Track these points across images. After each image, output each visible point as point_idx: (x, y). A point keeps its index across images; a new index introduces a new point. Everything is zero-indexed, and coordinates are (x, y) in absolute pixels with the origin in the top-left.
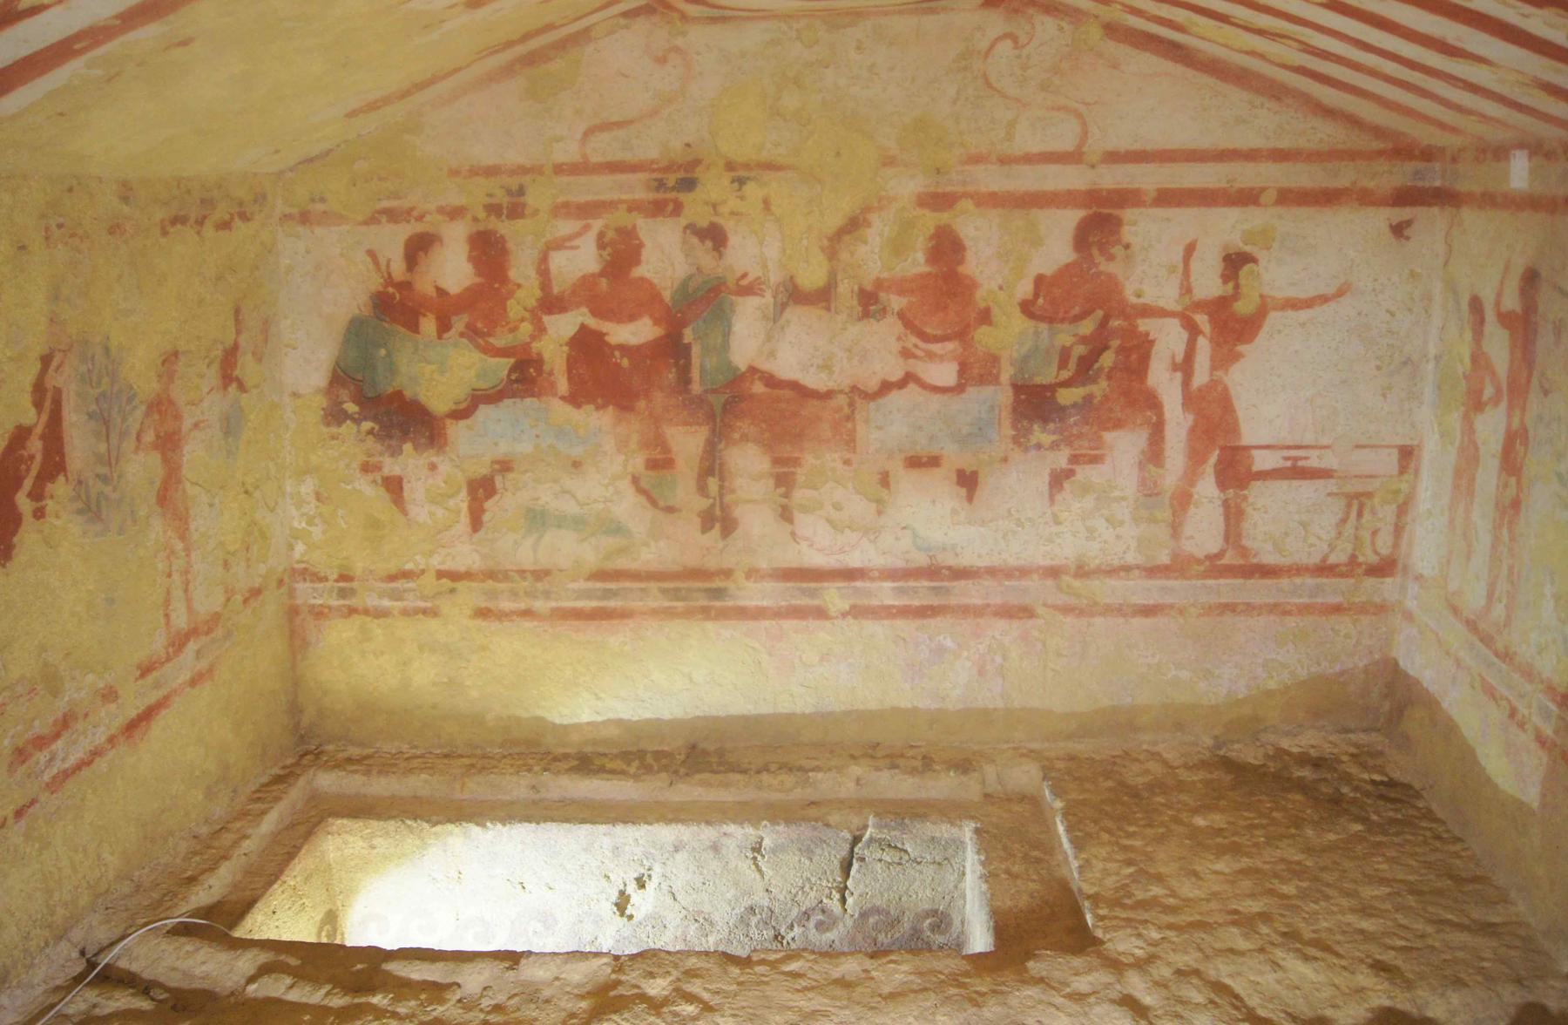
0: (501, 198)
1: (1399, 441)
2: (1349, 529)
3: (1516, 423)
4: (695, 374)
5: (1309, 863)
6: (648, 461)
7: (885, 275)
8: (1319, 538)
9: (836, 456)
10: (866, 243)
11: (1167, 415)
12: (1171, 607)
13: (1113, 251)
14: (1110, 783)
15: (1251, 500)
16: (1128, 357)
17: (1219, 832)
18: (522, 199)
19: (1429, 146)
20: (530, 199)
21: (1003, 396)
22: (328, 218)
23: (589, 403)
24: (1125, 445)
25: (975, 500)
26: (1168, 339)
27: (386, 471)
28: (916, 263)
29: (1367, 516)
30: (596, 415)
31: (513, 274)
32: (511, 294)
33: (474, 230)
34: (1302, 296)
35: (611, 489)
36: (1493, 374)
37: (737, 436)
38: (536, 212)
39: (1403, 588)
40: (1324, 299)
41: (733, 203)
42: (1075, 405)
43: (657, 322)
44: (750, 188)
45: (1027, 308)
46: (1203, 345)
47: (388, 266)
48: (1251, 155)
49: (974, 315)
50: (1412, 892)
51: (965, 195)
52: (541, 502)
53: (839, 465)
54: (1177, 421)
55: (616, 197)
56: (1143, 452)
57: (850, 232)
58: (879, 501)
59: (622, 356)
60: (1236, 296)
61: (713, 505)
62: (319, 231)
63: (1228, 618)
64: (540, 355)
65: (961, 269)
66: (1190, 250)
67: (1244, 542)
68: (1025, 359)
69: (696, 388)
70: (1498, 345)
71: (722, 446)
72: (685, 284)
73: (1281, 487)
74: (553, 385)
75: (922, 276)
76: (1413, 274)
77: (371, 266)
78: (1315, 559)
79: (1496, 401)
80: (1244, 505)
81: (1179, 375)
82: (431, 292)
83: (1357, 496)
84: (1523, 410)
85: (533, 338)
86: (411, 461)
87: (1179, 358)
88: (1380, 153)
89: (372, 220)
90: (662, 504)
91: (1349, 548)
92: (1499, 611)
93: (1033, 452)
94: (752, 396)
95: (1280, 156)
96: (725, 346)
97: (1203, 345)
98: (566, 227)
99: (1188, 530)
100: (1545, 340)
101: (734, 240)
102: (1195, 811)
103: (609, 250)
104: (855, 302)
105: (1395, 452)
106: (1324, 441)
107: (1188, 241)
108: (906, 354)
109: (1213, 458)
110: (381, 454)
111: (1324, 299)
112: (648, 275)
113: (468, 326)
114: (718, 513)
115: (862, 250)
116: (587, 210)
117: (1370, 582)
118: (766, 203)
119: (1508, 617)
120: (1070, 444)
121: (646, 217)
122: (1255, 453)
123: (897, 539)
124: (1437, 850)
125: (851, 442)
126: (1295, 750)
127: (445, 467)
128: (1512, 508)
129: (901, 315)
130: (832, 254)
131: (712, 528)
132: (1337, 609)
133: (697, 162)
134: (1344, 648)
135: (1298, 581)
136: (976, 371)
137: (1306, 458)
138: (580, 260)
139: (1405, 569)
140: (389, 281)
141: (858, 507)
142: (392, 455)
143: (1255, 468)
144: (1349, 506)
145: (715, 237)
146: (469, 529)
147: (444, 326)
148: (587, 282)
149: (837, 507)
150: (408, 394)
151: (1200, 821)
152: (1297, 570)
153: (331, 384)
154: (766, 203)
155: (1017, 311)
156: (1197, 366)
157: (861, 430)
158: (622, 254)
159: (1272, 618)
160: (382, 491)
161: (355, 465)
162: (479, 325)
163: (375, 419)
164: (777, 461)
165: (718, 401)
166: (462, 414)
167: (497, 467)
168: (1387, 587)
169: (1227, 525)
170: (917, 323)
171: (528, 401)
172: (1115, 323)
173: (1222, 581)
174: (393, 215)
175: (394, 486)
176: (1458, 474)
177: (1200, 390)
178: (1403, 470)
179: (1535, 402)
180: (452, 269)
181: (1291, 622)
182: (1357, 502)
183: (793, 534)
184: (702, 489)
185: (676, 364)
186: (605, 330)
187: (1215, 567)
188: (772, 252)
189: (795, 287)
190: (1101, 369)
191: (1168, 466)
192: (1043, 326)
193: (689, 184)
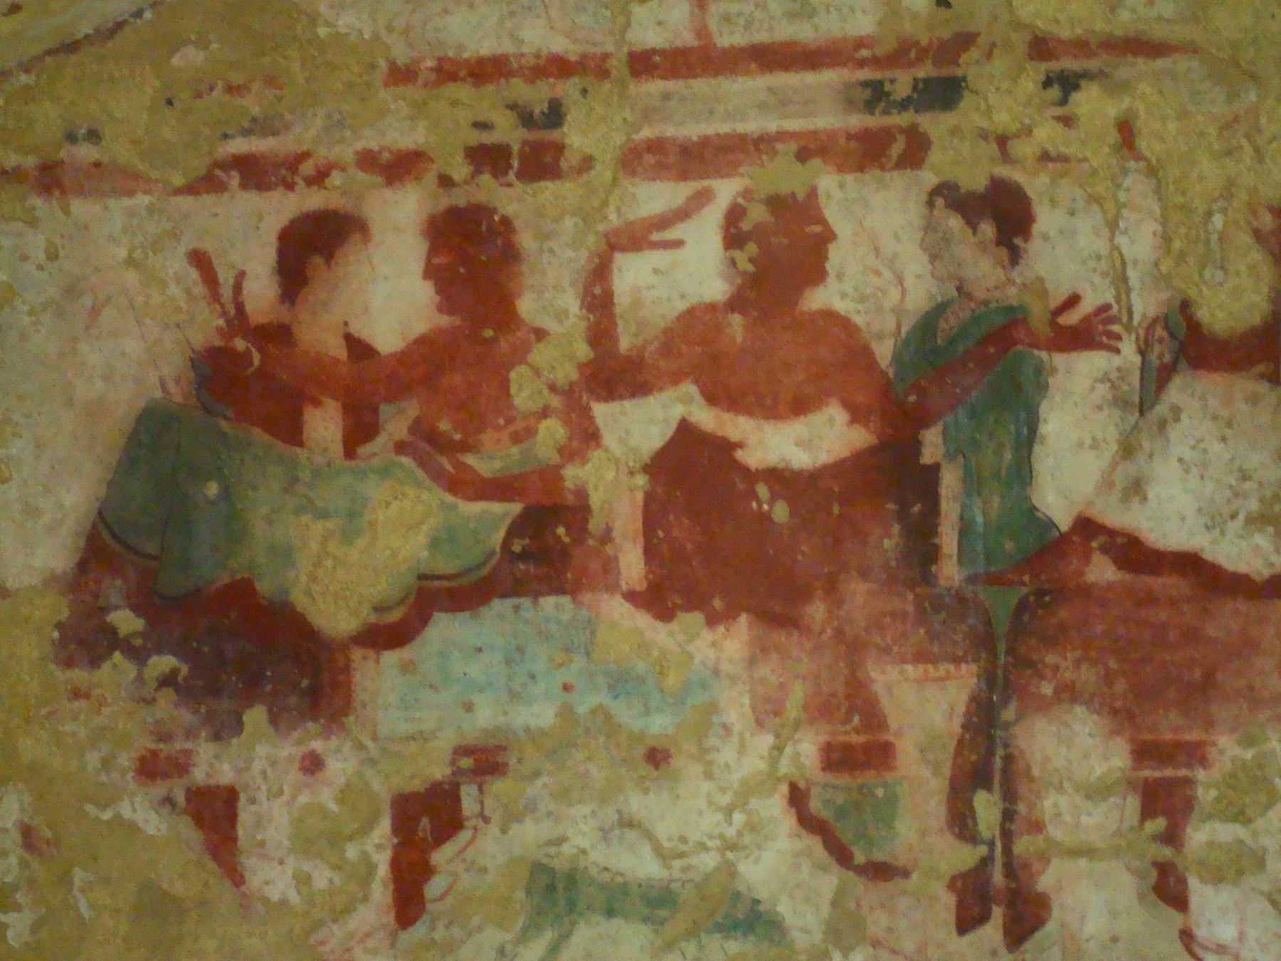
0: (507, 132)
4: (948, 540)
6: (828, 748)
18: (555, 135)
20: (576, 136)
22: (107, 179)
23: (690, 607)
27: (199, 775)
30: (707, 636)
31: (527, 306)
32: (520, 355)
33: (444, 202)
35: (738, 818)
37: (1047, 689)
38: (587, 163)
41: (1046, 133)
43: (857, 415)
44: (1088, 100)
47: (238, 288)
52: (567, 849)
55: (772, 126)
59: (774, 498)
61: (986, 862)
62: (78, 206)
64: (582, 494)
69: (950, 572)
71: (1008, 714)
72: (929, 322)
74: (610, 566)
77: (199, 289)
82: (337, 349)
85: (570, 454)
86: (262, 750)
89: (208, 183)
90: (859, 858)
94: (1087, 592)
96: (1023, 472)
98: (654, 197)
101: (1046, 220)
103: (752, 248)
110: (190, 734)
112: (841, 306)
113: (415, 428)
114: (998, 877)
116: (696, 159)
118: (1126, 130)
121: (841, 169)
127: (341, 766)
131: (983, 918)
133: (965, 40)
138: (686, 272)
140: (238, 320)
142: (217, 737)
145: (1005, 214)
146: (390, 918)
147: (360, 431)
148: (697, 323)
150: (265, 586)
153: (82, 565)
154: (1126, 130)
158: (781, 254)
160: (186, 827)
161: (125, 760)
162: (444, 426)
163: (180, 650)
164: (1144, 752)
165: (1002, 603)
166: (389, 634)
167: (466, 762)
171: (548, 602)
174: (254, 173)
175: (216, 814)
180: (389, 295)
183: (1187, 936)
184: (961, 822)
185: (902, 515)
186: (733, 434)
188: (1140, 244)
189: (1194, 327)
193: (944, 93)
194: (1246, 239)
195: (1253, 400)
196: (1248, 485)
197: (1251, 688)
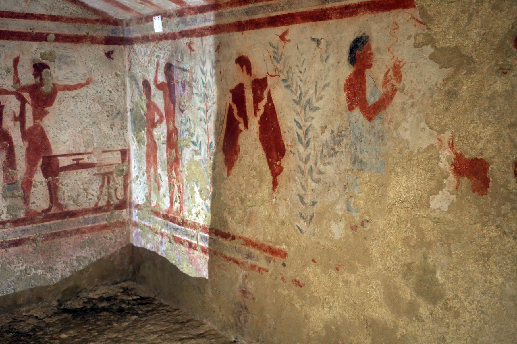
1: (120, 148)
2: (105, 190)
3: (171, 127)
5: (120, 336)
11: (15, 143)
12: (28, 239)
14: (11, 334)
15: (60, 181)
17: (75, 337)
19: (116, 19)
29: (112, 183)
34: (72, 84)
36: (158, 110)
39: (130, 213)
40: (81, 86)
46: (28, 107)
48: (40, 17)
50: (166, 333)
54: (20, 147)
56: (4, 162)
60: (41, 84)
63: (57, 240)
66: (16, 61)
67: (60, 201)
70: (159, 99)
76: (117, 75)
78: (93, 205)
79: (160, 121)
80: (57, 184)
81: (18, 123)
83: (106, 174)
84: (174, 121)
87: (17, 114)
88: (97, 21)
91: (106, 197)
92: (177, 205)
95: (54, 19)
99: (32, 199)
100: (178, 89)
102: (61, 332)
105: (119, 152)
106: (89, 150)
107: (15, 57)
109: (40, 163)
117: (117, 212)
119: (181, 207)
122: (59, 158)
124: (169, 316)
126: (96, 297)
128: (174, 163)
132: (105, 227)
134: (110, 243)
135: (86, 217)
137: (83, 159)
139: (130, 203)
143: (61, 165)
144: (104, 179)
151: (64, 336)
152: (86, 211)
156: (27, 118)
159: (77, 236)
168: (124, 212)
173: (52, 222)
176: (148, 156)
177: (29, 129)
178: (123, 160)
179: (178, 117)
181: (86, 236)
182: (106, 177)
187: (47, 215)
191: (18, 168)
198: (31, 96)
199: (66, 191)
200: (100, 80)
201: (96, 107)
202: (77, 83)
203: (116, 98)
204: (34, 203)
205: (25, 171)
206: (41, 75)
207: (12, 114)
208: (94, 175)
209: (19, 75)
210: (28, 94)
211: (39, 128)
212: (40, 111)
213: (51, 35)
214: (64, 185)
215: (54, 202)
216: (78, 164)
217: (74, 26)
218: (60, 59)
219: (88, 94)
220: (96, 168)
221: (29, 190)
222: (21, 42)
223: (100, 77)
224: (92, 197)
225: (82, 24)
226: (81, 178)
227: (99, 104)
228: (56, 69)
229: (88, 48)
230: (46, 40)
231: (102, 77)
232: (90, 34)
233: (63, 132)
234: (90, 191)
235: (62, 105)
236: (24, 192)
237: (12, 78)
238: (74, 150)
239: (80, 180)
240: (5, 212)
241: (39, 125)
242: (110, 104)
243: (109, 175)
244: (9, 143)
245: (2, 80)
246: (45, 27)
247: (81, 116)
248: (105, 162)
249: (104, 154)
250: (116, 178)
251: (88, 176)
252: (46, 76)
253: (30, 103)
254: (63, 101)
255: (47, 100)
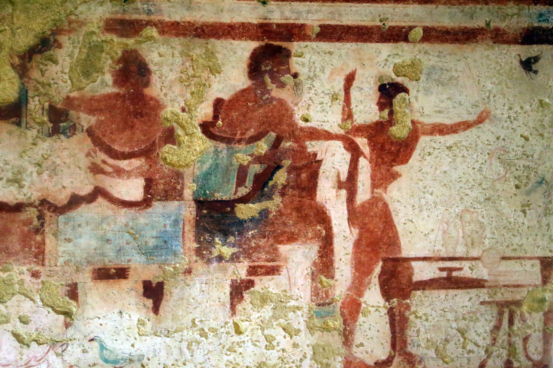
2: (502, 337)
7: (74, 94)
8: (476, 344)
9: (24, 268)
10: (56, 62)
11: (335, 230)
13: (282, 79)
15: (413, 309)
16: (298, 175)
21: (187, 210)
24: (299, 257)
25: (161, 311)
26: (334, 159)
28: (105, 84)
29: (516, 321)
34: (448, 122)
40: (467, 125)
42: (252, 219)
45: (207, 128)
46: (364, 164)
49: (159, 134)
51: (149, 23)
53: (27, 278)
57: (40, 52)
58: (67, 314)
60: (391, 122)
65: (147, 91)
66: (350, 80)
67: (409, 349)
68: (207, 176)
73: (439, 297)
75: (109, 97)
80: (407, 313)
81: (344, 192)
83: (507, 304)
87: (344, 177)
91: (505, 353)
93: (215, 264)
97: (364, 164)
99: (358, 338)
104: (46, 119)
105: (538, 262)
106: (475, 253)
108: (95, 169)
109: (378, 270)
111: (467, 125)
115: (53, 69)
120: (249, 256)
122: (414, 264)
123: (84, 351)
125: (40, 255)
129: (90, 132)
130: (22, 71)
136: (160, 189)
137: (460, 269)
141: (47, 320)
143: (417, 277)
144: (501, 314)
149: (24, 321)
155: (198, 132)
156: (359, 184)
157: (50, 241)
169: (393, 332)
170: (106, 140)
172: (287, 144)
177: (363, 206)
182: (507, 311)
190: (274, 186)
191: (337, 275)
192: (222, 146)
194: (9, 68)
195: (10, 133)
196: (7, 166)
197: (7, 248)
198: (369, 144)
199: (422, 330)
200: (506, 116)
201: (493, 167)
202: (459, 120)
203: (537, 152)
204: (362, 345)
205: (349, 283)
206: (391, 105)
207: (335, 175)
208: (482, 303)
209: (353, 106)
210: (365, 140)
211: (380, 205)
212: (383, 171)
213: (416, 29)
214: (421, 318)
215: (398, 348)
216: (449, 279)
217: (462, 11)
218: (429, 74)
219: (479, 142)
220: (485, 290)
221: (355, 319)
222: (360, 44)
223: (506, 108)
224: (475, 349)
225: (479, 6)
226: (455, 308)
227: (501, 162)
228: (420, 95)
229: (487, 53)
230: (406, 40)
231: (511, 109)
232: (492, 25)
233: (425, 213)
234: (471, 335)
235: (425, 163)
236: (345, 322)
237: (340, 111)
238: (444, 250)
239: (452, 310)
240: (309, 356)
241: (381, 199)
242: (522, 163)
243: (513, 307)
244: (325, 229)
245: (323, 114)
246: (406, 15)
247: (461, 184)
248: (502, 280)
249: (504, 262)
250: (527, 315)
251: (468, 303)
252: (400, 107)
253: (368, 156)
254: (430, 154)
255: (399, 151)
